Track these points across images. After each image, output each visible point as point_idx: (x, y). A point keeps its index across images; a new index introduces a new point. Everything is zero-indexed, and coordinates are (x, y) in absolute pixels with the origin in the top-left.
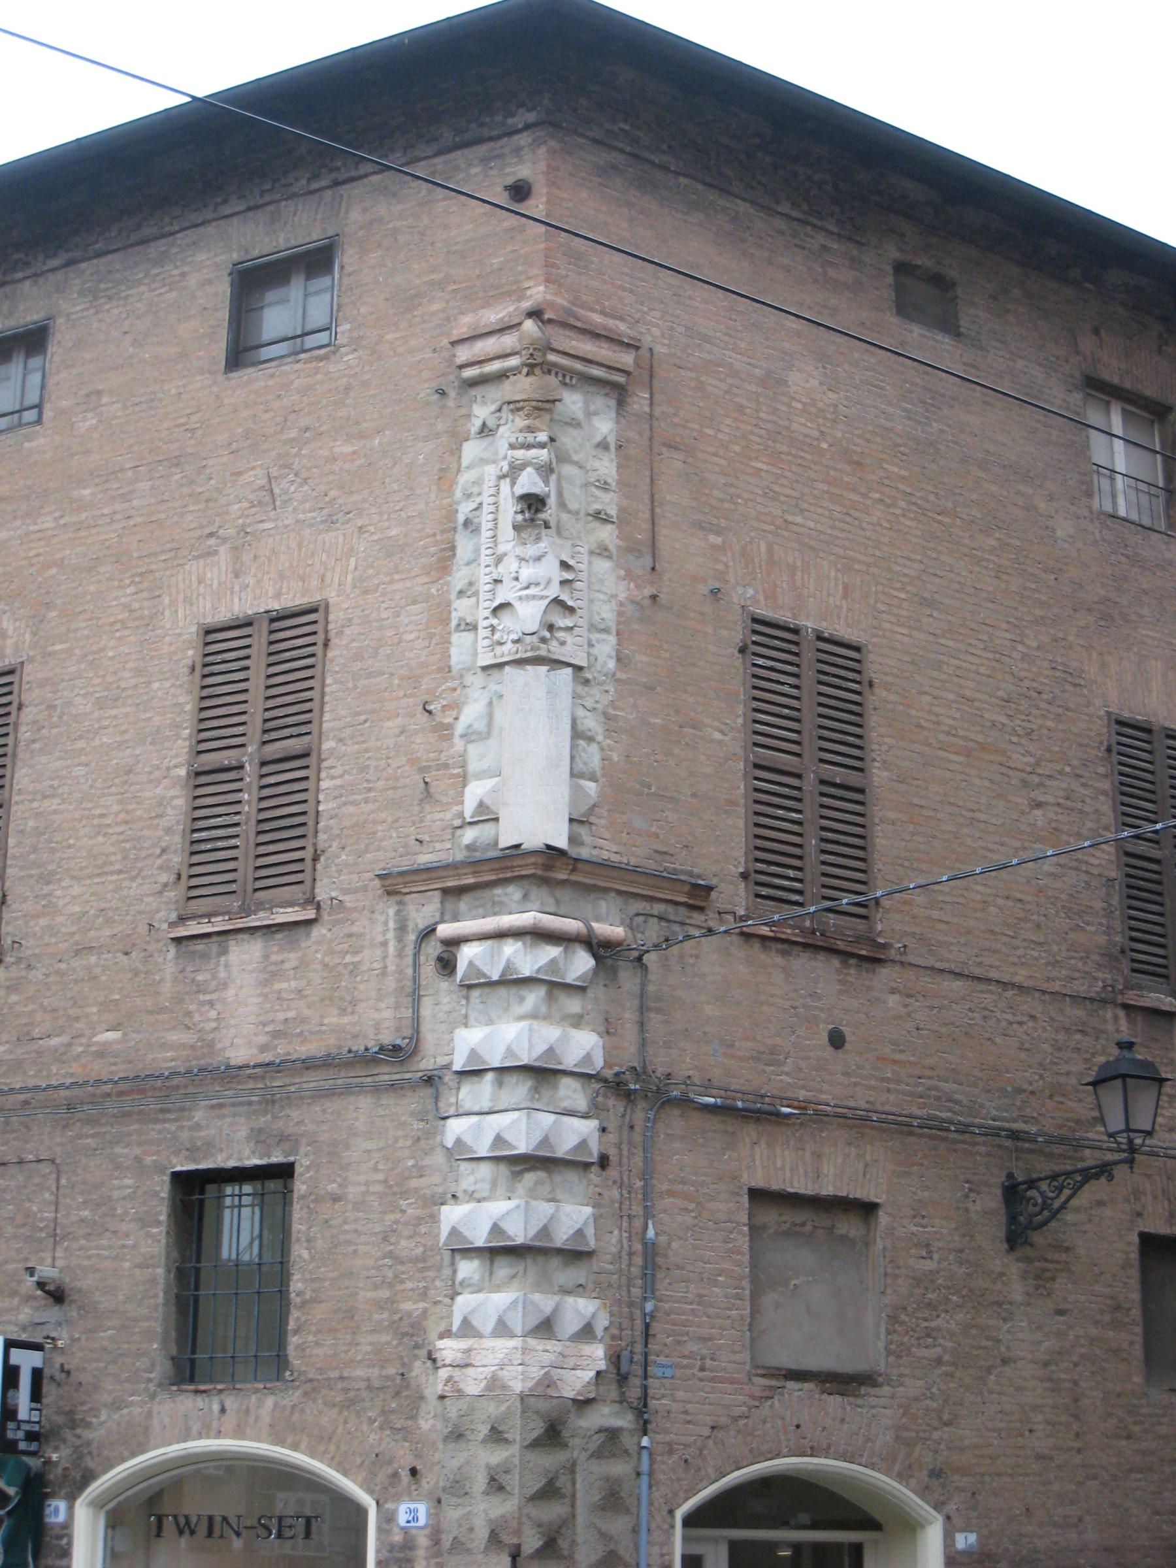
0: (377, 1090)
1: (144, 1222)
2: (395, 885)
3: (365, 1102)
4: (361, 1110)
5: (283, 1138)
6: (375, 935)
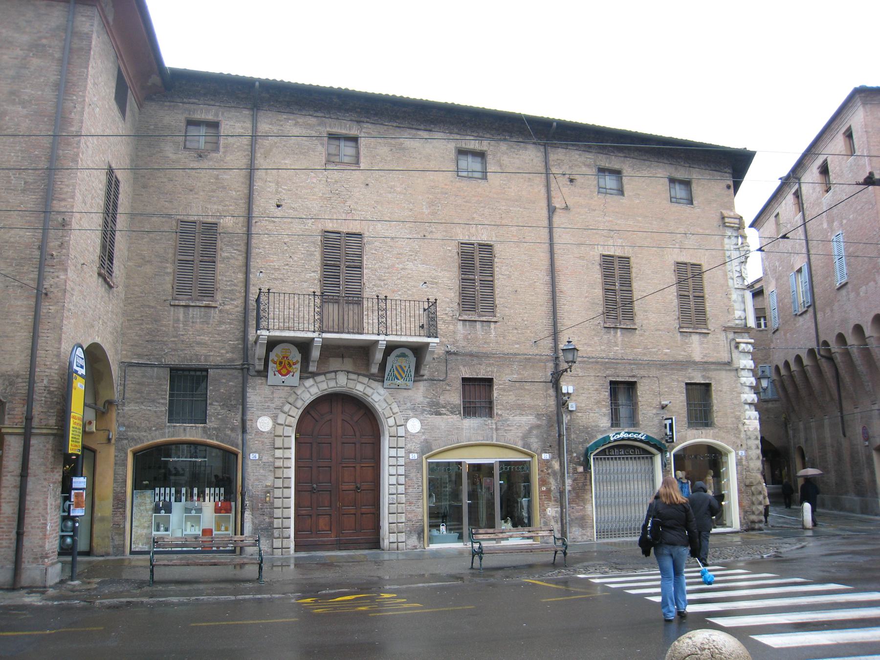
0: (726, 370)
1: (681, 393)
2: (726, 329)
3: (724, 372)
4: (723, 374)
5: (708, 378)
6: (722, 339)
